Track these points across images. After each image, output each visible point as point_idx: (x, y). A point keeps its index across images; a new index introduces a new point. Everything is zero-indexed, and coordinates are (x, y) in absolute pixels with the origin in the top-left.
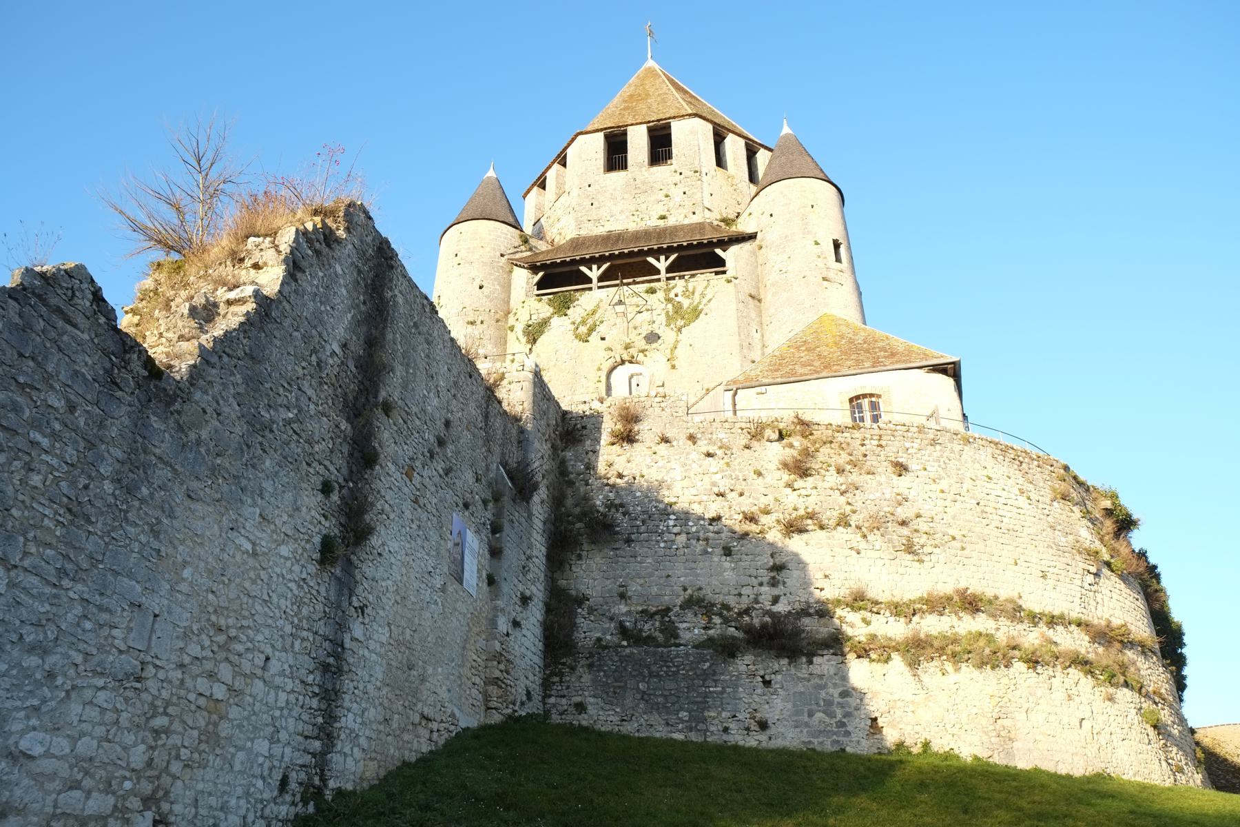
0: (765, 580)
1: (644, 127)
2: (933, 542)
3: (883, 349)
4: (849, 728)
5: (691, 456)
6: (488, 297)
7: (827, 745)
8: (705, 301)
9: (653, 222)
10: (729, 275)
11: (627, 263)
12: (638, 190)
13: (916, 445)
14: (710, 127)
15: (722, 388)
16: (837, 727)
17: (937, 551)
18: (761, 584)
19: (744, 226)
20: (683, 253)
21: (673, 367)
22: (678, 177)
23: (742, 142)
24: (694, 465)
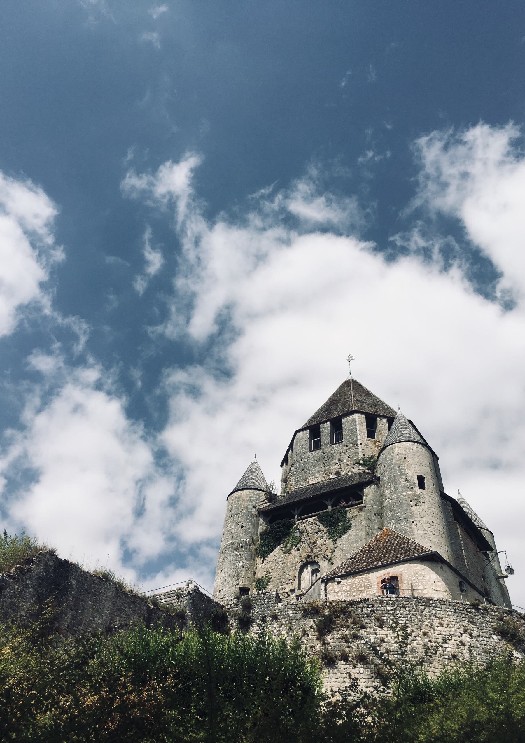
1: (329, 423)
3: (403, 549)
5: (275, 626)
6: (245, 532)
12: (326, 458)
14: (365, 416)
15: (320, 581)
21: (332, 563)
22: (345, 448)
23: (385, 421)
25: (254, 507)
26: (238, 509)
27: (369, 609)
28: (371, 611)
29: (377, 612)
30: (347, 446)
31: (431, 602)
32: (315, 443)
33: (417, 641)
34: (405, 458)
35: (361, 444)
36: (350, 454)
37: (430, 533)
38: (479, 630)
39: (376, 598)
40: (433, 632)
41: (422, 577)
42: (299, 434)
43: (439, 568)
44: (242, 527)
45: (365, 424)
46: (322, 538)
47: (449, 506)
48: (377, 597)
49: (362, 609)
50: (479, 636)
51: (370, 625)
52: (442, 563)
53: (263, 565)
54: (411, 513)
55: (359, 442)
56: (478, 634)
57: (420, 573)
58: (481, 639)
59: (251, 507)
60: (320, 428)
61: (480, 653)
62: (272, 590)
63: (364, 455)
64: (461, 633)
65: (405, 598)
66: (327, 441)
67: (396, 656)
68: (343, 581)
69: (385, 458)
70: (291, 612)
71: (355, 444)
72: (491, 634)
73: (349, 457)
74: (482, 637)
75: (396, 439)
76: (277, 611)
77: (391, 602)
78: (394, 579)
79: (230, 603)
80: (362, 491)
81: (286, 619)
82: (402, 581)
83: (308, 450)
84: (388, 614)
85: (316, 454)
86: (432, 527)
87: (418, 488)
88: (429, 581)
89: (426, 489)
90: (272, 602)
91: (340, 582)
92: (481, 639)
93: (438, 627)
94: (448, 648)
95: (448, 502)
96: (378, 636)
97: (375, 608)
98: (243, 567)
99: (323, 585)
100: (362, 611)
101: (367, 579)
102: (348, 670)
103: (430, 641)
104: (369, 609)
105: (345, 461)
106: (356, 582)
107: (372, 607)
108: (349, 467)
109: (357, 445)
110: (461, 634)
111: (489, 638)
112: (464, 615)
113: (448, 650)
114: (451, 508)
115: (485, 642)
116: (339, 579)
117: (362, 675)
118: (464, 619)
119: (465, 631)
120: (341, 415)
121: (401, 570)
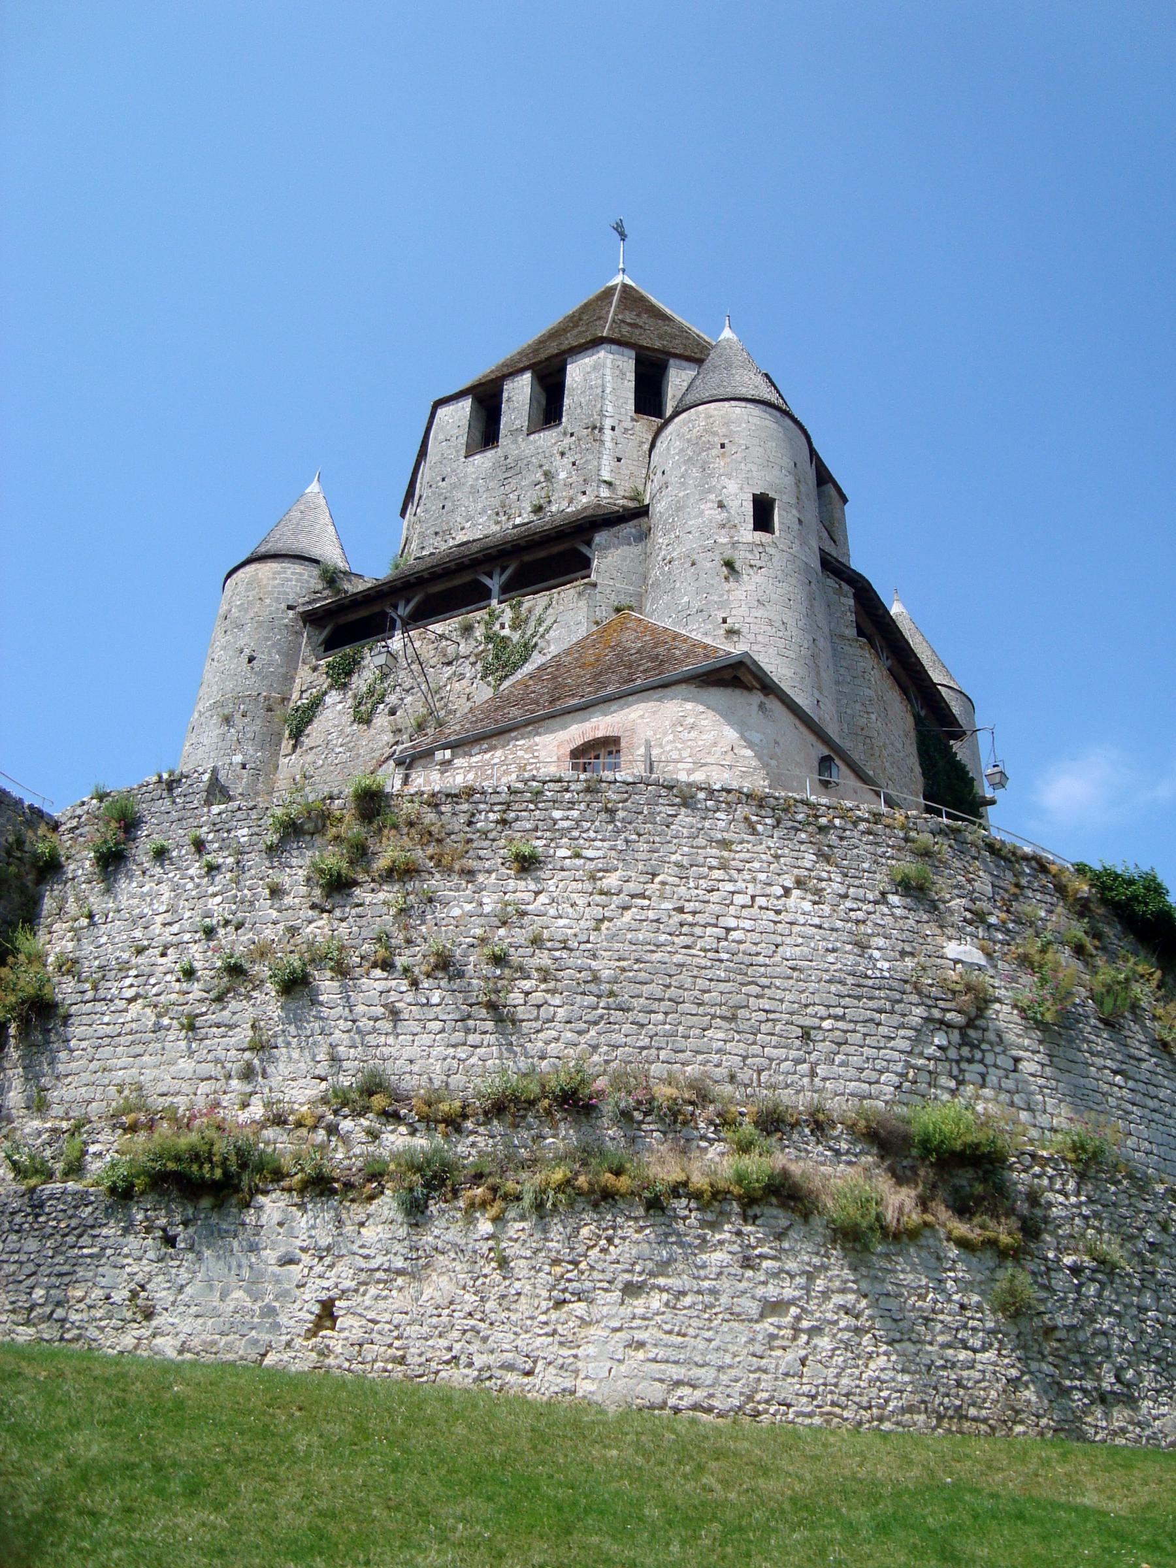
0: (234, 1068)
2: (552, 985)
4: (283, 1319)
5: (191, 872)
7: (238, 1349)
8: (541, 630)
9: (523, 516)
10: (593, 577)
11: (444, 587)
12: (510, 469)
14: (633, 354)
16: (263, 1315)
17: (557, 1000)
18: (229, 1077)
19: (619, 500)
20: (527, 558)
22: (568, 440)
24: (190, 886)
25: (290, 608)
26: (246, 611)
28: (497, 822)
30: (572, 435)
31: (701, 795)
32: (486, 431)
33: (634, 910)
34: (723, 446)
35: (613, 429)
36: (577, 456)
37: (772, 651)
38: (849, 880)
39: (520, 785)
40: (692, 885)
41: (693, 734)
42: (442, 412)
43: (755, 708)
44: (251, 660)
46: (462, 677)
47: (846, 596)
48: (526, 782)
49: (473, 815)
50: (845, 896)
51: (487, 864)
52: (766, 695)
53: (293, 757)
54: (721, 596)
55: (608, 423)
56: (842, 891)
57: (690, 720)
58: (849, 904)
59: (283, 606)
60: (501, 391)
61: (839, 945)
62: (201, 770)
63: (619, 460)
64: (783, 886)
65: (616, 781)
67: (557, 954)
68: (458, 762)
69: (668, 449)
70: (245, 831)
71: (596, 428)
72: (883, 894)
73: (574, 464)
75: (706, 395)
76: (205, 829)
77: (568, 796)
78: (608, 746)
79: (79, 812)
80: (589, 543)
81: (226, 853)
82: (631, 746)
83: (463, 453)
85: (484, 460)
86: (780, 634)
87: (752, 526)
88: (715, 744)
89: (777, 533)
90: (196, 804)
91: (450, 762)
92: (849, 904)
93: (710, 868)
94: (734, 929)
95: (845, 587)
96: (507, 897)
97: (512, 815)
98: (244, 767)
100: (470, 824)
101: (526, 751)
102: (393, 997)
103: (681, 910)
105: (563, 475)
106: (496, 761)
107: (504, 812)
108: (571, 492)
109: (601, 430)
110: (787, 892)
111: (876, 903)
112: (803, 836)
113: (734, 935)
114: (852, 602)
115: (860, 915)
116: (448, 753)
117: (435, 1009)
118: (803, 848)
119: (799, 883)
120: (564, 352)
121: (633, 716)
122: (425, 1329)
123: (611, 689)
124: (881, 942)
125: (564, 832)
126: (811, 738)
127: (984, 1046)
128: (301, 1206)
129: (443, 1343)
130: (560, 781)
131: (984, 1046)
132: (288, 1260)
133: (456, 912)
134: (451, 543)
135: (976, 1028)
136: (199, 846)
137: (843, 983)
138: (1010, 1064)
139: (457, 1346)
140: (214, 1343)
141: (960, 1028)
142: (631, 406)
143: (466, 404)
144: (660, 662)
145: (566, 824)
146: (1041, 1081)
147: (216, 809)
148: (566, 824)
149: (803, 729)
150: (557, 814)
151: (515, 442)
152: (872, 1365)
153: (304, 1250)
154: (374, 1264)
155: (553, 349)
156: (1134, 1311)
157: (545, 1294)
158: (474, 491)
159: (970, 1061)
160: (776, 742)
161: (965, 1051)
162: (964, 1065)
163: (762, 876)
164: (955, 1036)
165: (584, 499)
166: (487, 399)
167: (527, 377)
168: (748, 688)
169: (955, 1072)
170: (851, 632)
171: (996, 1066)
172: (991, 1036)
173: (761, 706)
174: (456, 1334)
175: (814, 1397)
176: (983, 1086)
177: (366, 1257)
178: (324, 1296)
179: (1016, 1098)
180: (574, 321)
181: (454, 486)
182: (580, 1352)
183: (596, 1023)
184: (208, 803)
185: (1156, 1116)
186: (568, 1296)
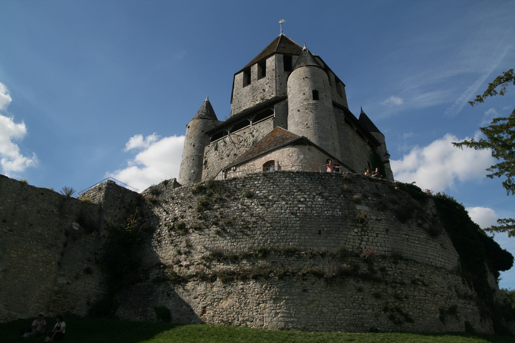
1: (257, 64)
13: (260, 182)
14: (282, 56)
27: (240, 185)
29: (247, 186)
32: (247, 81)
42: (236, 76)
43: (307, 149)
45: (283, 62)
48: (248, 175)
57: (291, 154)
66: (255, 78)
74: (332, 197)
84: (255, 186)
85: (248, 88)
95: (341, 110)
99: (224, 173)
103: (287, 204)
104: (240, 185)
105: (267, 90)
115: (334, 200)
122: (228, 312)
123: (272, 148)
124: (339, 207)
125: (258, 187)
126: (324, 155)
127: (368, 231)
128: (198, 284)
129: (232, 315)
130: (256, 174)
131: (368, 231)
132: (196, 298)
133: (233, 209)
134: (241, 110)
135: (365, 227)
136: (173, 198)
137: (329, 218)
138: (375, 235)
139: (235, 316)
140: (179, 318)
141: (361, 227)
142: (283, 70)
143: (242, 73)
144: (284, 140)
145: (258, 185)
146: (385, 239)
147: (176, 189)
148: (258, 185)
149: (321, 153)
150: (256, 183)
151: (255, 82)
152: (338, 315)
153: (199, 295)
154: (215, 297)
155: (263, 57)
156: (412, 297)
157: (255, 302)
158: (246, 96)
159: (364, 235)
160: (313, 158)
161: (363, 233)
162: (363, 237)
163: (308, 193)
164: (360, 229)
165: (273, 96)
166: (247, 72)
167: (257, 64)
168: (305, 144)
169: (360, 238)
170: (343, 122)
171: (371, 236)
172: (370, 228)
173: (309, 149)
174: (234, 313)
175: (323, 324)
176: (368, 241)
177: (214, 296)
178: (204, 306)
179: (378, 244)
180: (269, 47)
181: (241, 96)
182: (264, 316)
183: (267, 234)
184: (174, 187)
185: (418, 245)
186: (261, 302)
